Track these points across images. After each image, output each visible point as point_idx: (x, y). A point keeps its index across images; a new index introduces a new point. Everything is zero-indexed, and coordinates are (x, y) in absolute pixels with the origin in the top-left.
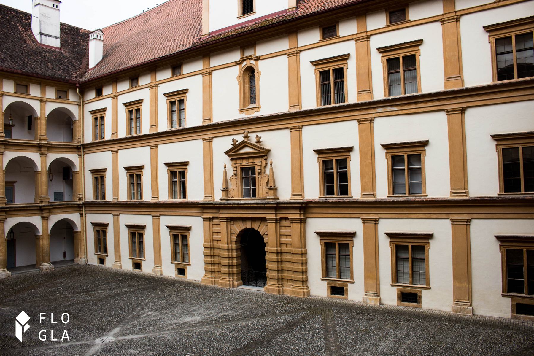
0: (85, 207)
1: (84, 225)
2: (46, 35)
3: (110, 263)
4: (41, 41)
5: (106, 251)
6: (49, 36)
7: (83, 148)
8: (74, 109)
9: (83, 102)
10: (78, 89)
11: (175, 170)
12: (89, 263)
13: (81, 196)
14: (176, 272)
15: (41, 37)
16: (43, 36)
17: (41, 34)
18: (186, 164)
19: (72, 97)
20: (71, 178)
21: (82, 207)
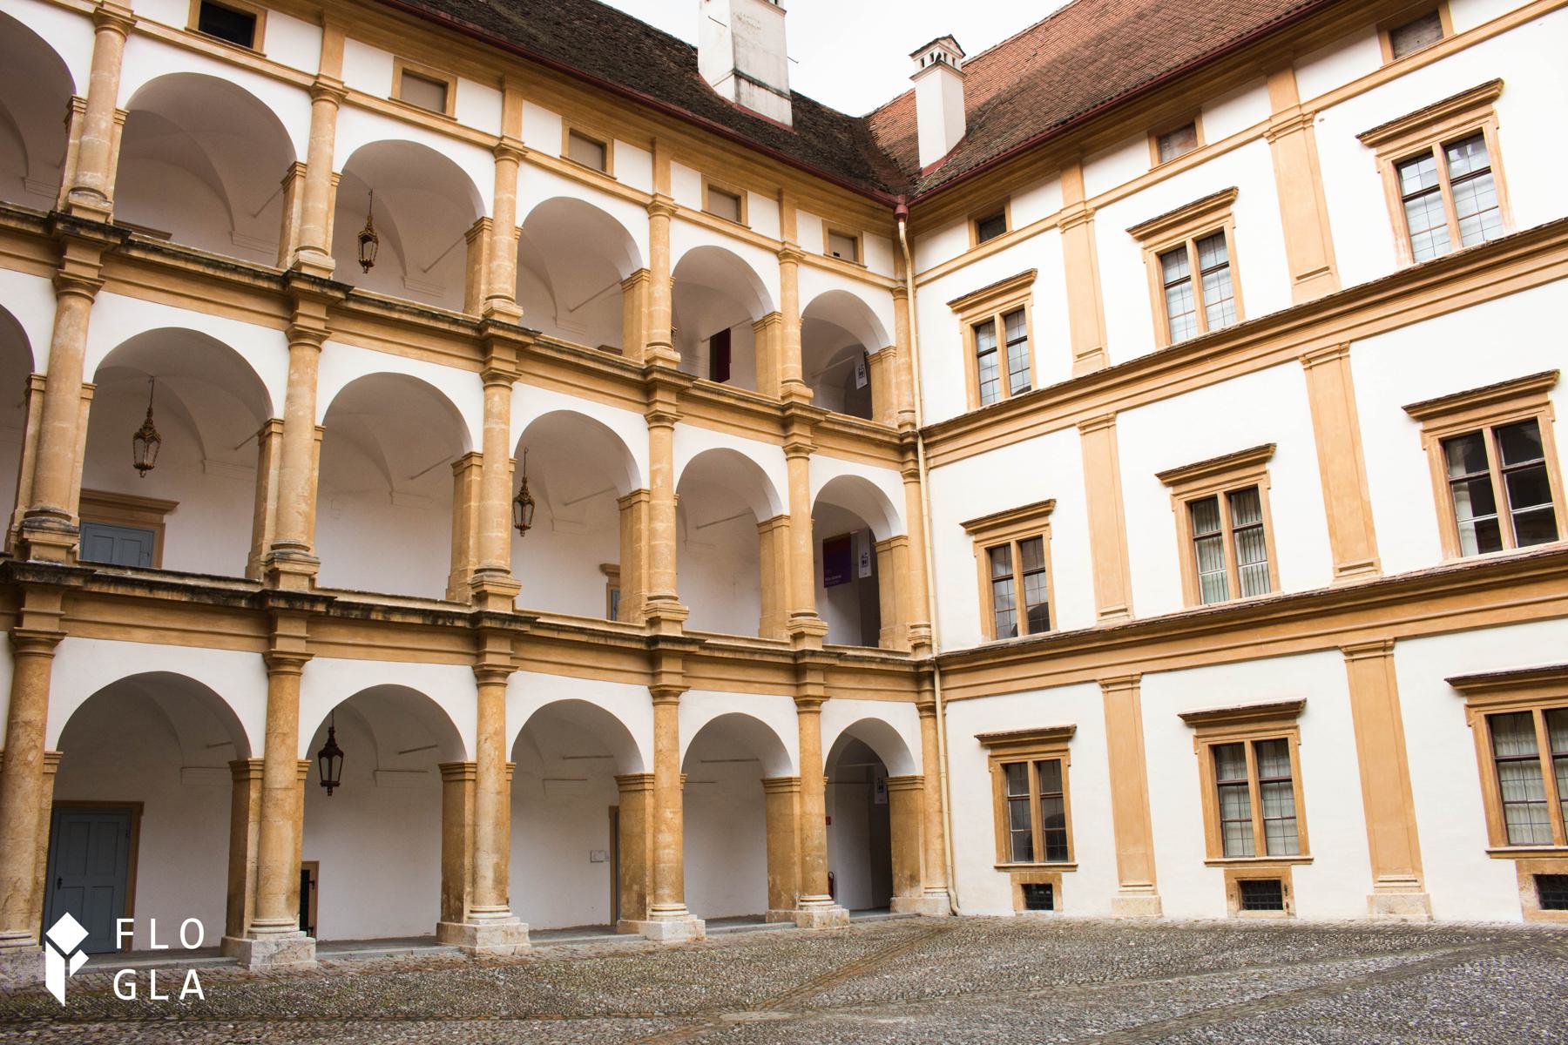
0: (943, 675)
1: (937, 751)
2: (752, 81)
3: (1088, 893)
4: (738, 95)
5: (1058, 846)
6: (761, 85)
7: (926, 446)
8: (880, 304)
9: (915, 277)
10: (902, 225)
11: (1472, 427)
12: (964, 911)
13: (923, 631)
14: (1532, 896)
15: (738, 84)
16: (744, 83)
17: (738, 75)
18: (1543, 383)
19: (873, 257)
20: (864, 572)
21: (931, 676)
